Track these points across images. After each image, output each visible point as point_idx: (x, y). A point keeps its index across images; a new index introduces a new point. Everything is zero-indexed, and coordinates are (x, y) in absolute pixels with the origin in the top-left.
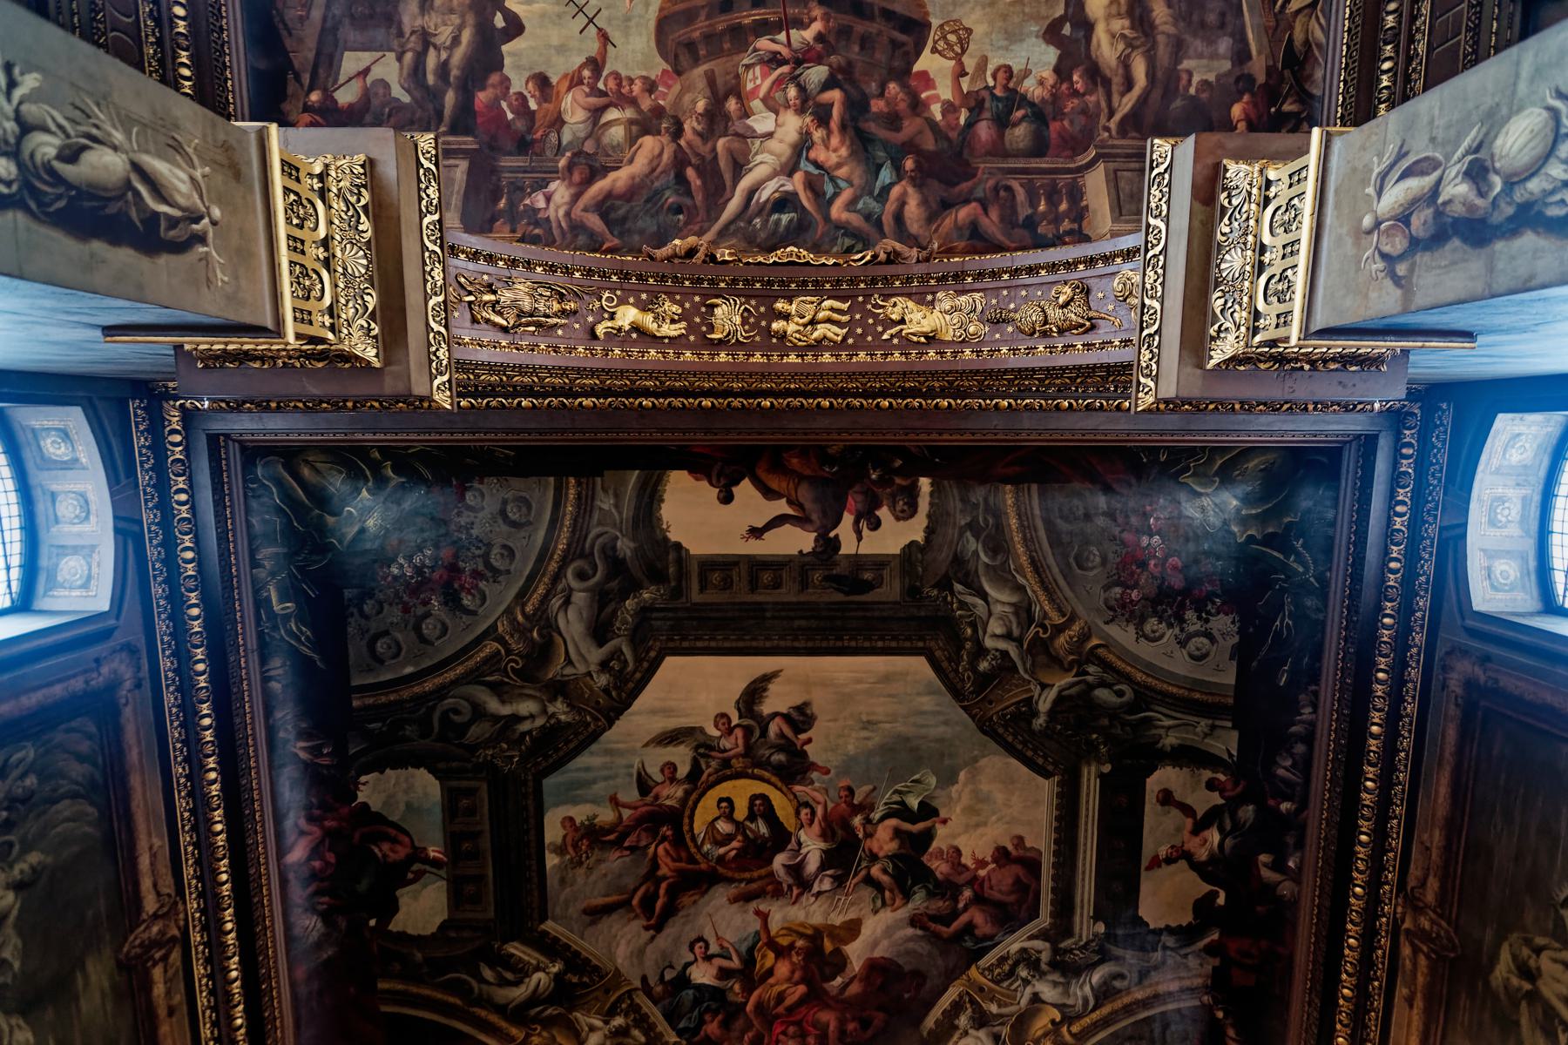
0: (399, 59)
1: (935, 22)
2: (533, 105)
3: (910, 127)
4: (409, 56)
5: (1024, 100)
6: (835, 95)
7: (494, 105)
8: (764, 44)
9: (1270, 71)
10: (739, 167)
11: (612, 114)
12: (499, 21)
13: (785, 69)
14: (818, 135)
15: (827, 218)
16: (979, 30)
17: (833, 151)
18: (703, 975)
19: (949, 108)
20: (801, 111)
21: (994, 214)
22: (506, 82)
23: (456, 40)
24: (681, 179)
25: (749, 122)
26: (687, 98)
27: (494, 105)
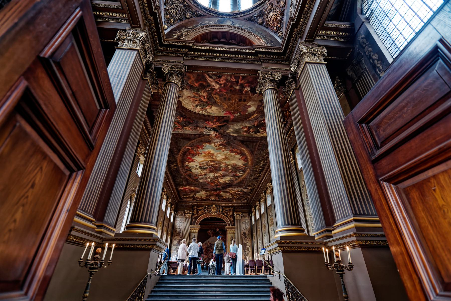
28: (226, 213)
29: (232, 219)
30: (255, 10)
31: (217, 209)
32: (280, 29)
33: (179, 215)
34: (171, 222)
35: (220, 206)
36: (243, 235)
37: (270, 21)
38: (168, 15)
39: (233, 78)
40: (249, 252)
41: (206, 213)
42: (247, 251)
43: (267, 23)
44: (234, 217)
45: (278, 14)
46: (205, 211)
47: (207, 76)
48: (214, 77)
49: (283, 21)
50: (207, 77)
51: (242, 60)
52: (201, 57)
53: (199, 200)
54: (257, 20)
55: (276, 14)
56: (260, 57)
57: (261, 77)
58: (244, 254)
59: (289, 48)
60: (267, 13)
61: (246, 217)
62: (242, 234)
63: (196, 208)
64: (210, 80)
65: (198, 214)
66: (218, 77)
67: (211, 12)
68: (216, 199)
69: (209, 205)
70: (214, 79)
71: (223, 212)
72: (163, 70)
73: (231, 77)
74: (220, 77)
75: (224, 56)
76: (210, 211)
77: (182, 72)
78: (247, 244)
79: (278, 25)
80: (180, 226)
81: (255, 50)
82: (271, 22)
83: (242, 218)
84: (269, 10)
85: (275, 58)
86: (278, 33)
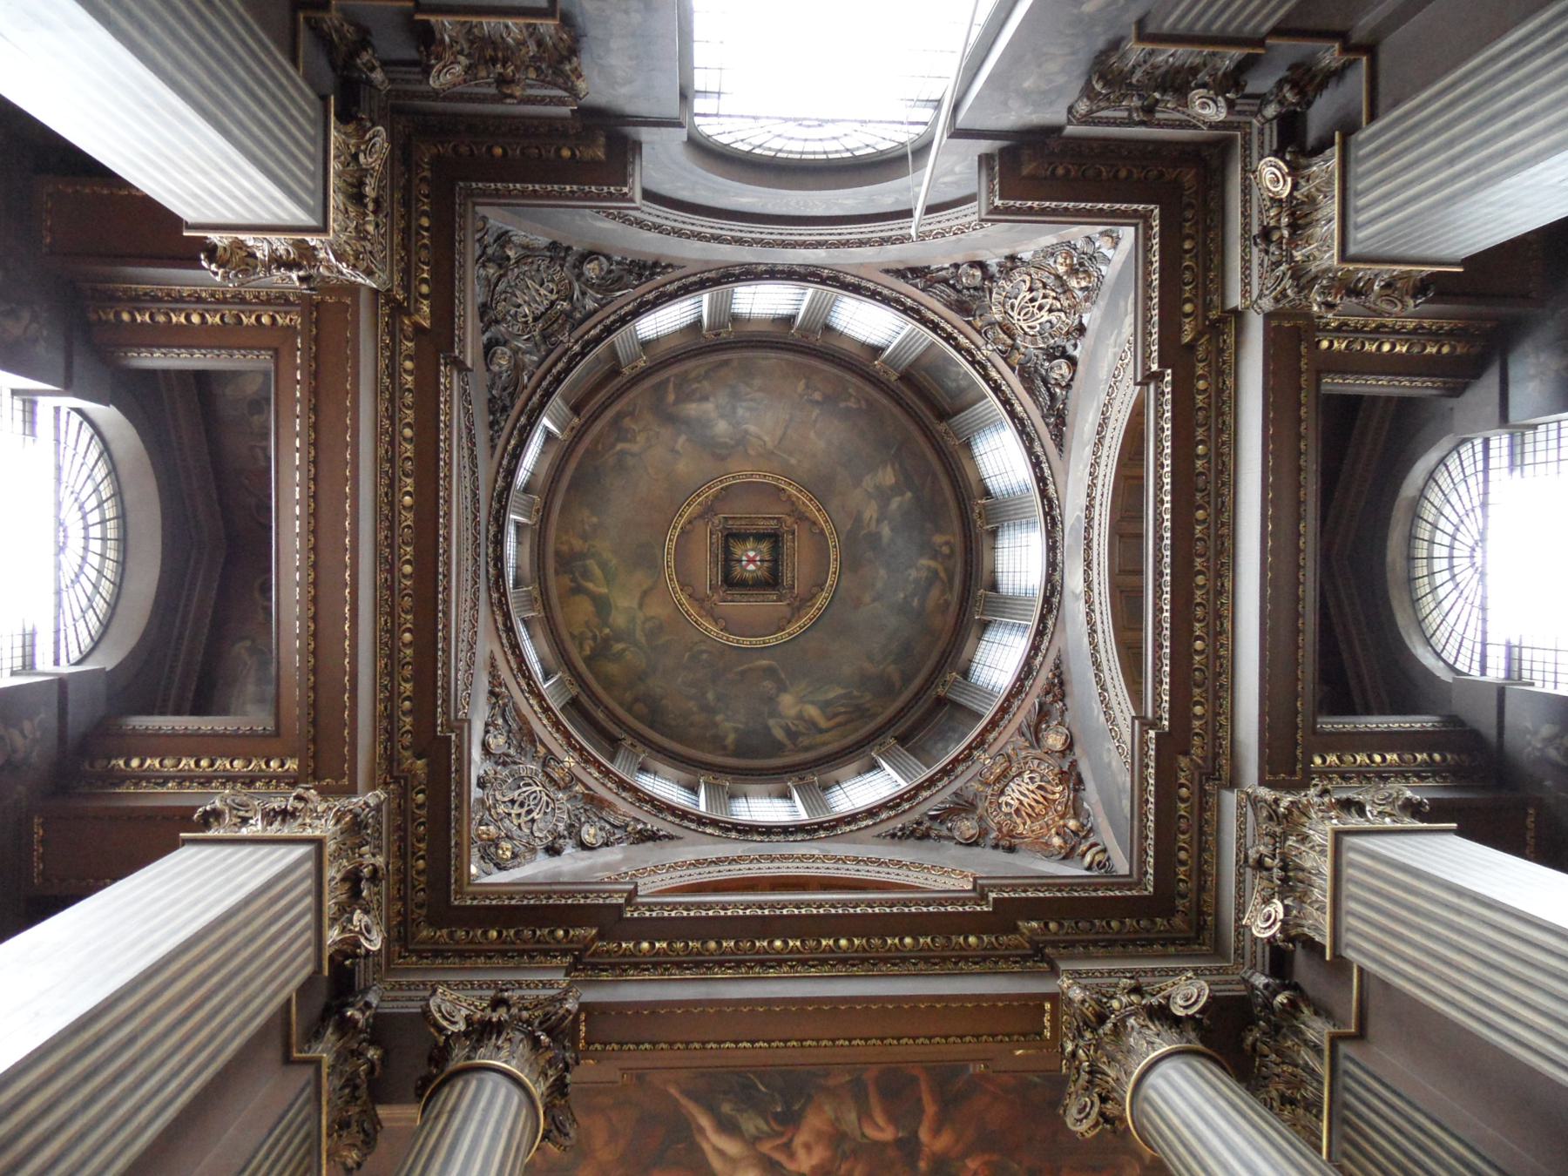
30: (926, 794)
32: (1085, 837)
37: (1019, 821)
38: (487, 825)
39: (881, 1120)
43: (1005, 830)
45: (1049, 782)
47: (704, 1121)
48: (751, 1124)
49: (1085, 805)
50: (701, 1130)
51: (926, 960)
52: (679, 965)
54: (950, 830)
55: (1040, 787)
56: (1032, 930)
57: (1083, 1001)
59: (1183, 863)
60: (990, 791)
64: (721, 1153)
66: (776, 1116)
67: (705, 824)
70: (753, 1142)
72: (438, 1015)
73: (865, 1114)
74: (790, 1120)
75: (812, 950)
77: (564, 1017)
79: (1065, 826)
81: (992, 895)
82: (1024, 824)
84: (998, 780)
85: (1118, 932)
86: (1083, 855)
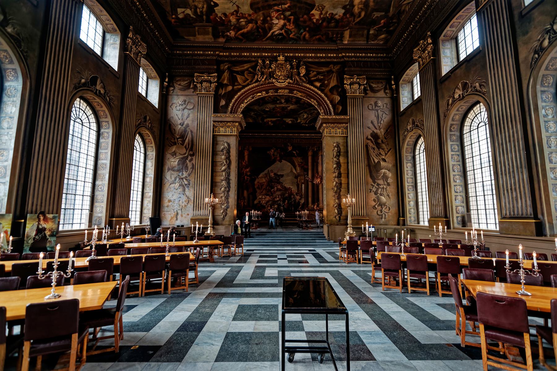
0: (191, 10)
1: (317, 5)
2: (224, 18)
3: (308, 23)
4: (193, 10)
5: (335, 19)
6: (292, 17)
7: (215, 18)
8: (276, 8)
9: (393, 15)
10: (271, 28)
11: (242, 20)
12: (212, 3)
13: (281, 12)
14: (288, 24)
15: (289, 37)
16: (327, 6)
17: (291, 27)
18: (267, 109)
19: (317, 20)
20: (284, 20)
21: (324, 37)
22: (217, 15)
23: (203, 7)
24: (258, 31)
25: (273, 21)
26: (258, 17)
27: (215, 18)
28: (318, 80)
29: (337, 98)
31: (292, 67)
33: (177, 87)
34: (143, 100)
35: (299, 62)
36: (369, 141)
40: (388, 184)
41: (257, 81)
42: (381, 182)
44: (344, 91)
46: (254, 74)
53: (236, 38)
58: (374, 189)
61: (378, 91)
62: (367, 139)
63: (228, 68)
65: (233, 85)
68: (288, 32)
69: (268, 57)
71: (309, 78)
76: (271, 75)
78: (382, 163)
80: (185, 117)
83: (366, 94)
